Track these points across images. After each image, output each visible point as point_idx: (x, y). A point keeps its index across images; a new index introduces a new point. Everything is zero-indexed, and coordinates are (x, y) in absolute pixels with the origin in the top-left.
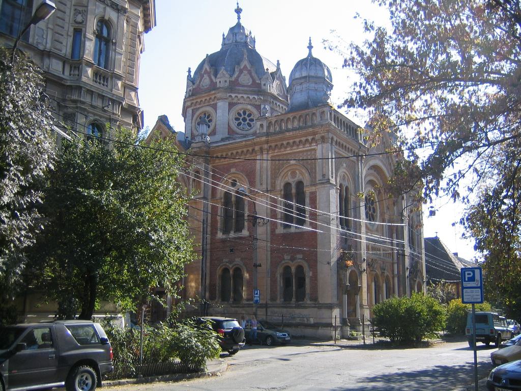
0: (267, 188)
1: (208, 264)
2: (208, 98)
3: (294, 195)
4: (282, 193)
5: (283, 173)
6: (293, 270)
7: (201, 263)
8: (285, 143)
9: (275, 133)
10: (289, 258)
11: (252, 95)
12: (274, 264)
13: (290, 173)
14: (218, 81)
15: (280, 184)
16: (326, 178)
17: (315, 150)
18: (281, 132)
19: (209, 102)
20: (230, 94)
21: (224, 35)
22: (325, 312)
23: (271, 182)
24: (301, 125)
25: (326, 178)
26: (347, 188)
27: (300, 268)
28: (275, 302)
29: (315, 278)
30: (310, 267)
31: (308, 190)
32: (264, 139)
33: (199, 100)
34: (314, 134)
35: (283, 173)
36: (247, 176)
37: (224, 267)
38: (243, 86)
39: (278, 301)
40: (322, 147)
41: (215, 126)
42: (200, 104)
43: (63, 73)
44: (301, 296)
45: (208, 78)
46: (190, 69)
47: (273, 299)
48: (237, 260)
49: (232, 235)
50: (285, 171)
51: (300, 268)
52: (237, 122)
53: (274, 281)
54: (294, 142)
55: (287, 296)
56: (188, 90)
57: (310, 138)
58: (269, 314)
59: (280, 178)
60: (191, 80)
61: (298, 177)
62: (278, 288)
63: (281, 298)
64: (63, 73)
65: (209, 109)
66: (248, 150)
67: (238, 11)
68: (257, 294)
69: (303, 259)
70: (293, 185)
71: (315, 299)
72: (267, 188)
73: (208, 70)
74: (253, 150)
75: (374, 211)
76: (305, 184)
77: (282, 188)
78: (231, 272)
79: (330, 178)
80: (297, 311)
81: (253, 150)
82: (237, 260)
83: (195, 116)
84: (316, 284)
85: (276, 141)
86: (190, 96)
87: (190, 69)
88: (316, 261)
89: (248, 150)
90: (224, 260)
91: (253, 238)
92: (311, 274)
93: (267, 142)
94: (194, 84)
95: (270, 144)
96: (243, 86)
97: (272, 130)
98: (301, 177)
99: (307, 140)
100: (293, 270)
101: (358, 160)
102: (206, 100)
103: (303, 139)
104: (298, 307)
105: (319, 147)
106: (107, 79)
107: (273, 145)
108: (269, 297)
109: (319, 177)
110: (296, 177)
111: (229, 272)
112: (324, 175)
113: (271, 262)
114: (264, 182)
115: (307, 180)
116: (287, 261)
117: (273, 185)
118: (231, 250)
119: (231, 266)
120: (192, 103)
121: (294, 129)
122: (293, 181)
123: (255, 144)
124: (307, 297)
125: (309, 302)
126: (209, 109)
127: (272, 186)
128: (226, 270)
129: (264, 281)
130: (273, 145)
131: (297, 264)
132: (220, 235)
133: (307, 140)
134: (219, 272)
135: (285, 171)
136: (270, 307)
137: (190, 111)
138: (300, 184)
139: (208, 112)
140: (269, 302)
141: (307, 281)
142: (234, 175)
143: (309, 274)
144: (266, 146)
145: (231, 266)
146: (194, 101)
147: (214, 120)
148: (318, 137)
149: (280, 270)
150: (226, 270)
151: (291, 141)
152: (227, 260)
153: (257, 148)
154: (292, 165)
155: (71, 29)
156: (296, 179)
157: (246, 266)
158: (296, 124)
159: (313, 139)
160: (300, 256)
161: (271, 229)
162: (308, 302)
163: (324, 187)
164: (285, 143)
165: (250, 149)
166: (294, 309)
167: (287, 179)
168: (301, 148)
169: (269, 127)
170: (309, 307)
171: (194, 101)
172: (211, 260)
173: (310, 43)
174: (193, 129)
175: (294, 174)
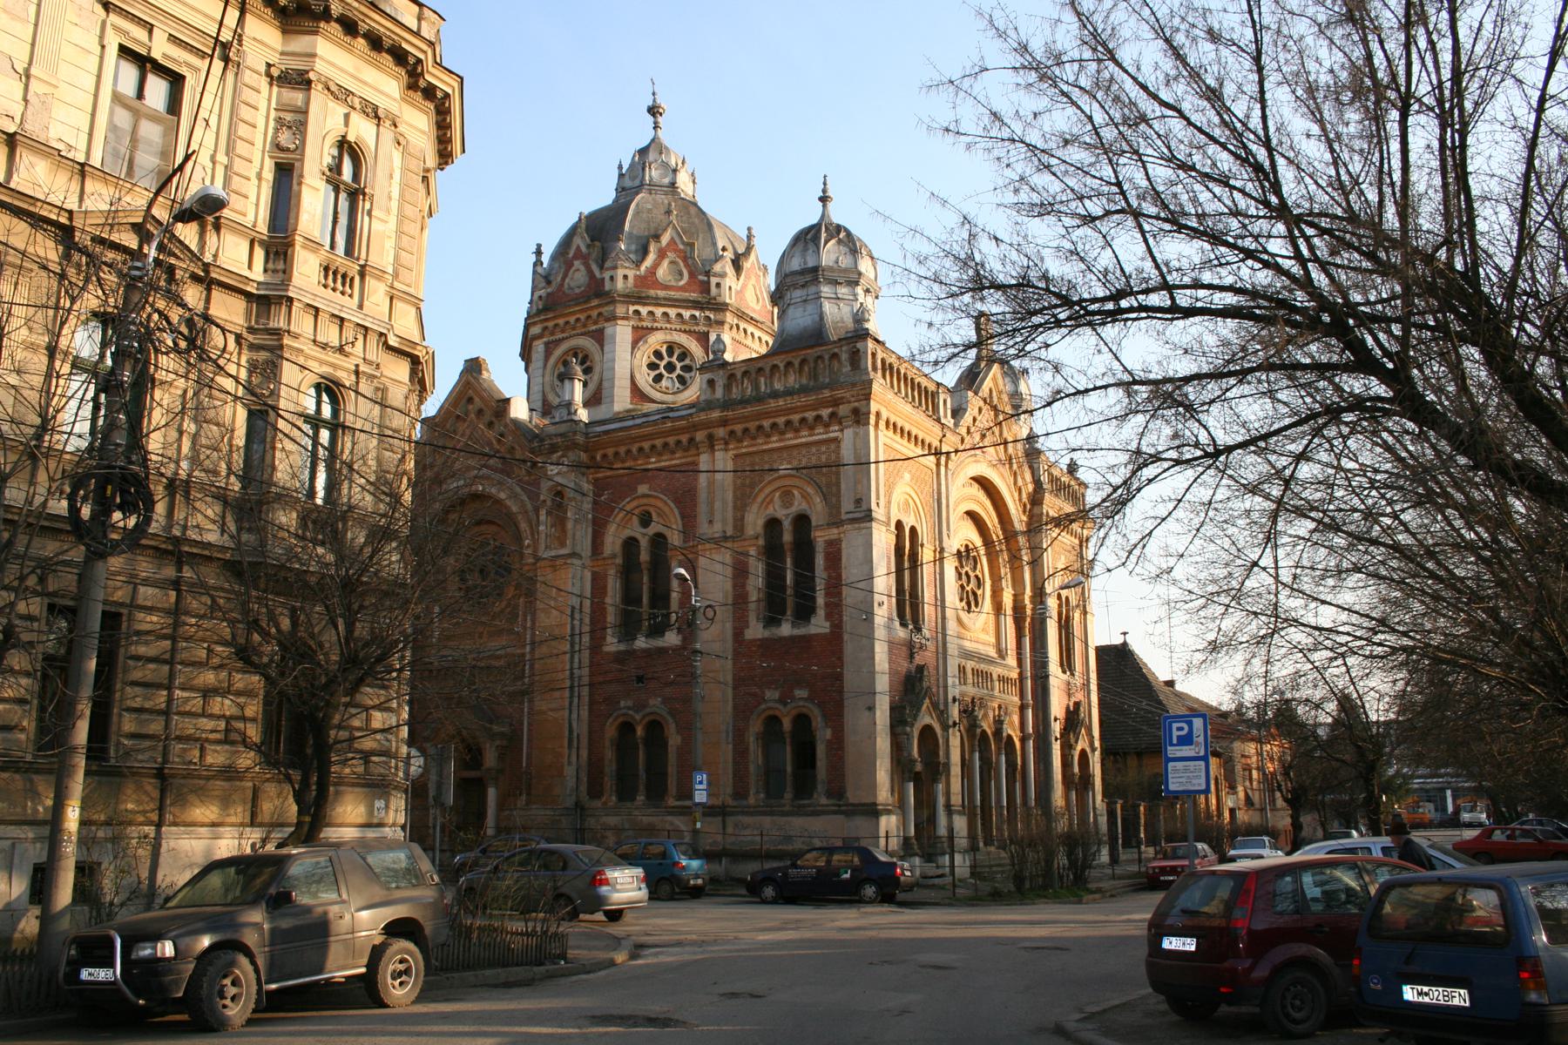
1: (585, 714)
2: (582, 317)
3: (787, 547)
4: (761, 542)
5: (762, 496)
6: (787, 724)
8: (766, 424)
9: (744, 402)
10: (776, 695)
11: (687, 308)
12: (742, 712)
14: (607, 275)
15: (755, 522)
16: (864, 507)
17: (836, 440)
18: (759, 399)
19: (585, 326)
20: (637, 307)
21: (620, 167)
23: (735, 520)
24: (804, 381)
25: (864, 507)
26: (913, 529)
27: (802, 721)
28: (744, 803)
29: (837, 745)
31: (820, 537)
32: (716, 414)
33: (561, 321)
34: (836, 402)
35: (762, 496)
36: (677, 501)
38: (667, 288)
39: (752, 801)
40: (856, 434)
41: (600, 384)
42: (563, 331)
43: (250, 267)
44: (804, 786)
45: (582, 268)
46: (539, 246)
47: (740, 793)
48: (651, 702)
49: (641, 643)
50: (767, 491)
51: (802, 721)
52: (653, 374)
53: (741, 753)
54: (788, 423)
55: (772, 786)
56: (537, 294)
57: (825, 413)
58: (730, 830)
59: (755, 507)
60: (542, 278)
61: (799, 505)
62: (752, 768)
64: (250, 267)
65: (586, 343)
66: (679, 442)
67: (654, 111)
69: (810, 699)
71: (837, 792)
73: (584, 249)
74: (691, 440)
75: (980, 583)
76: (814, 523)
78: (640, 731)
79: (874, 506)
80: (798, 823)
81: (691, 440)
82: (651, 702)
83: (552, 360)
84: (841, 758)
85: (746, 419)
86: (539, 312)
87: (539, 246)
88: (840, 705)
89: (679, 442)
90: (622, 704)
91: (687, 651)
92: (828, 734)
93: (724, 422)
94: (549, 283)
95: (730, 428)
96: (667, 288)
97: (736, 393)
98: (804, 506)
99: (818, 418)
100: (787, 724)
102: (578, 320)
103: (810, 415)
104: (799, 812)
105: (849, 433)
106: (352, 279)
107: (738, 428)
108: (729, 790)
109: (847, 505)
110: (792, 505)
111: (634, 731)
112: (858, 502)
113: (735, 707)
114: (718, 516)
115: (818, 512)
116: (771, 704)
117: (739, 524)
118: (640, 679)
121: (789, 393)
122: (785, 514)
123: (695, 427)
124: (820, 788)
125: (824, 801)
126: (586, 343)
127: (735, 527)
128: (627, 728)
130: (738, 428)
131: (794, 712)
132: (612, 644)
133: (818, 418)
134: (611, 731)
135: (767, 491)
136: (732, 814)
137: (539, 347)
138: (802, 521)
139: (582, 350)
140: (730, 802)
141: (821, 750)
142: (645, 501)
143: (823, 734)
144: (721, 432)
145: (638, 717)
147: (597, 370)
148: (843, 410)
149: (755, 727)
150: (627, 728)
151: (781, 420)
152: (630, 703)
153: (700, 436)
155: (269, 165)
156: (794, 509)
158: (792, 380)
159: (833, 415)
160: (801, 693)
161: (735, 628)
164: (766, 424)
165: (684, 438)
167: (770, 511)
168: (805, 437)
169: (728, 388)
171: (550, 324)
172: (592, 703)
173: (824, 191)
174: (548, 389)
175: (787, 496)
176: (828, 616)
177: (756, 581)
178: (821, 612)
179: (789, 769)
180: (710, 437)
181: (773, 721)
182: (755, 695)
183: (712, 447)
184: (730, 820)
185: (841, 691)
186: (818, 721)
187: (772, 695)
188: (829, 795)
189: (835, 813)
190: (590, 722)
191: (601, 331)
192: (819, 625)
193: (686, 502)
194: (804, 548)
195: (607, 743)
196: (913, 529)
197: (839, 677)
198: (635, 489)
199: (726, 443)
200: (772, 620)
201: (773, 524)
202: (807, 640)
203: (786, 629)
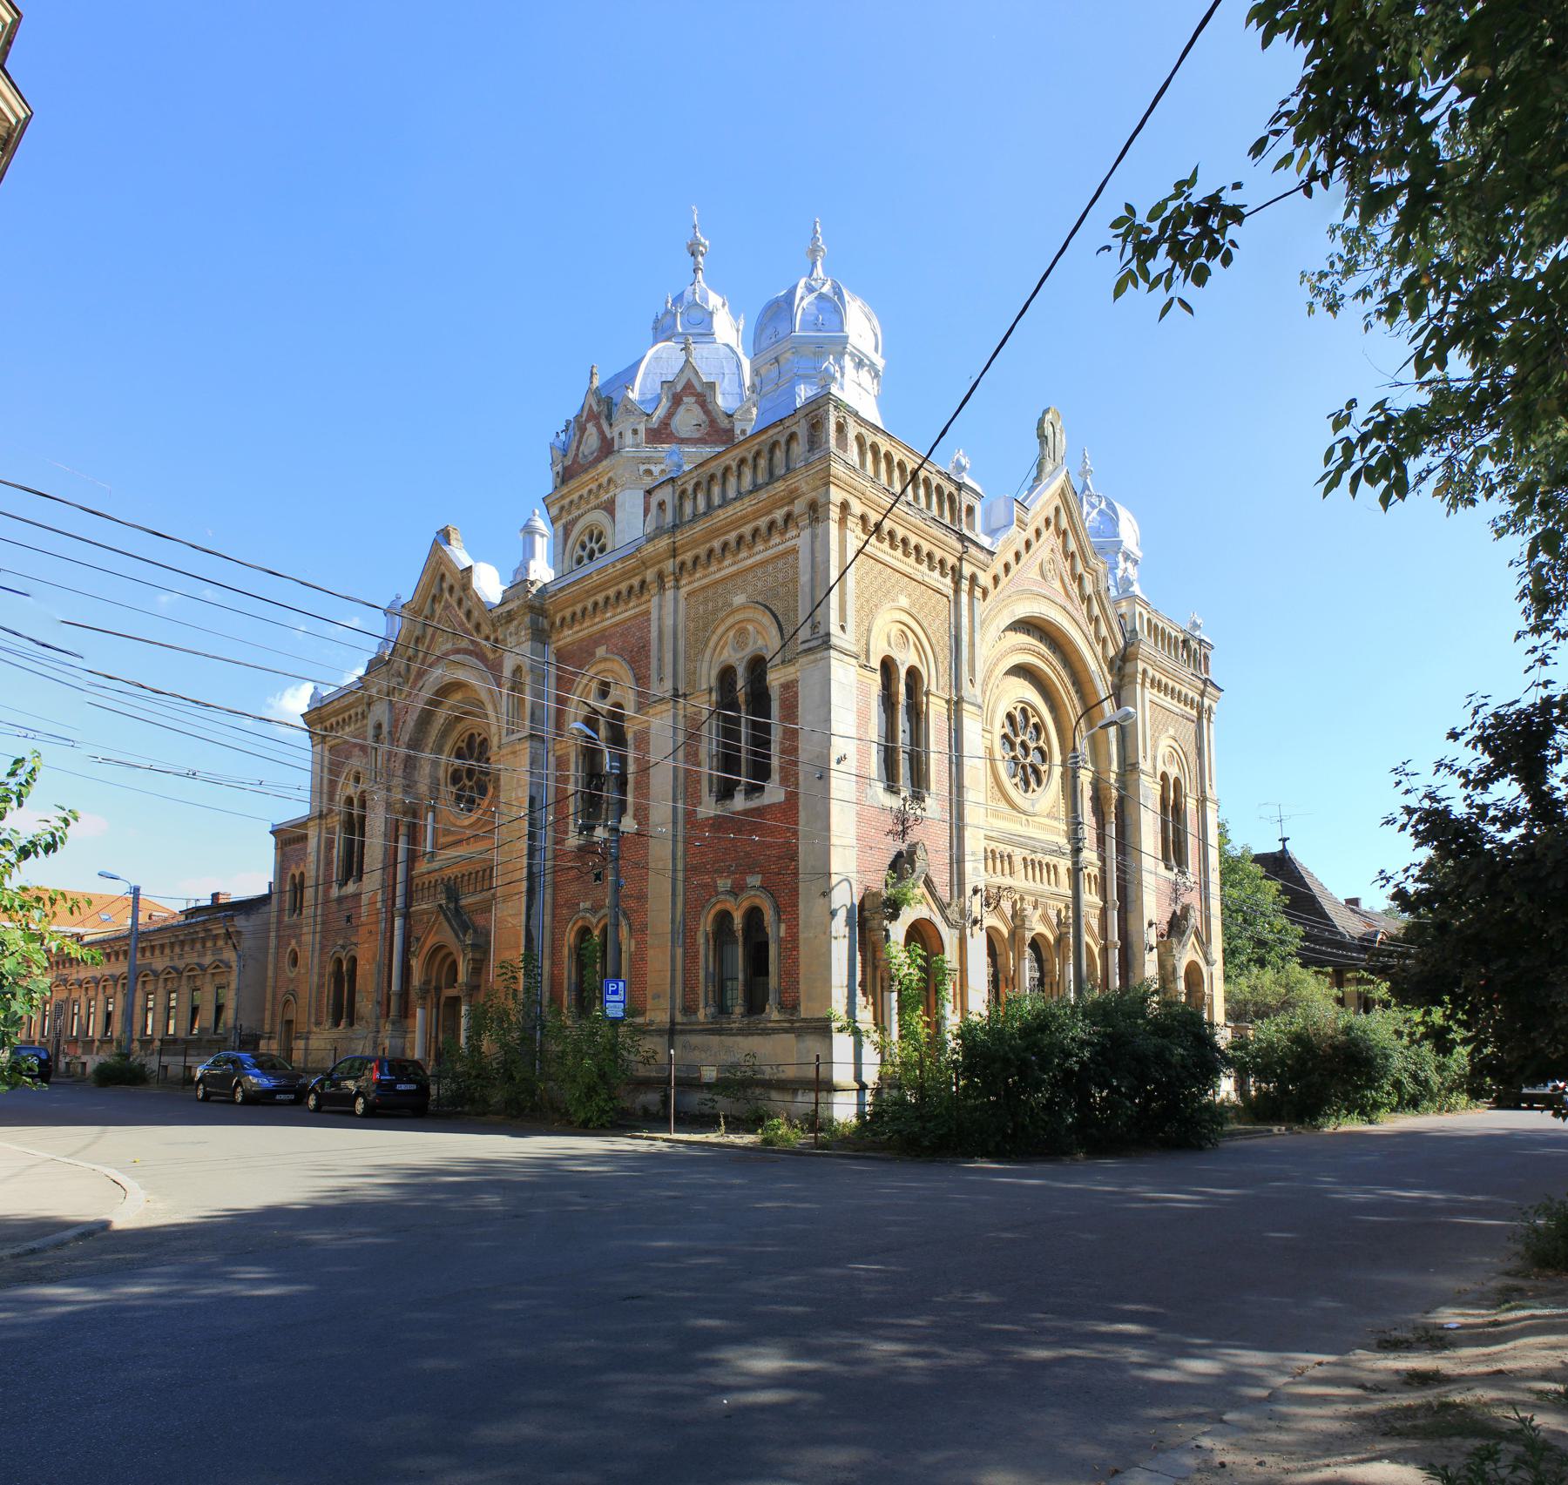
0: (676, 689)
5: (715, 638)
7: (523, 918)
12: (693, 908)
13: (731, 634)
22: (812, 1044)
26: (913, 673)
27: (754, 915)
28: (693, 1018)
29: (791, 944)
30: (778, 910)
31: (775, 679)
37: (580, 923)
39: (701, 1015)
50: (720, 631)
51: (754, 915)
53: (690, 957)
63: (706, 1005)
68: (615, 992)
70: (741, 671)
72: (676, 689)
77: (713, 682)
84: (796, 961)
88: (795, 892)
101: (957, 591)
104: (744, 1032)
119: (594, 921)
120: (562, 508)
122: (738, 659)
125: (775, 1016)
127: (688, 684)
129: (661, 963)
134: (570, 937)
135: (720, 631)
136: (683, 1032)
138: (758, 666)
140: (679, 1018)
143: (775, 930)
146: (566, 501)
149: (706, 924)
152: (588, 905)
154: (738, 610)
156: (748, 652)
157: (628, 919)
160: (754, 880)
162: (773, 1014)
163: (815, 661)
165: (636, 581)
166: (739, 1039)
170: (775, 1031)
172: (555, 906)
176: (784, 781)
177: (709, 745)
178: (775, 776)
179: (741, 977)
180: (661, 576)
181: (724, 918)
182: (706, 885)
183: (662, 587)
184: (679, 1039)
185: (796, 874)
186: (769, 916)
187: (724, 883)
188: (782, 1007)
189: (786, 1031)
190: (554, 928)
191: (612, 501)
192: (774, 793)
193: (637, 658)
194: (759, 699)
195: (566, 951)
196: (913, 673)
197: (793, 856)
198: (593, 654)
199: (677, 580)
200: (725, 791)
201: (727, 674)
202: (759, 812)
203: (739, 802)
